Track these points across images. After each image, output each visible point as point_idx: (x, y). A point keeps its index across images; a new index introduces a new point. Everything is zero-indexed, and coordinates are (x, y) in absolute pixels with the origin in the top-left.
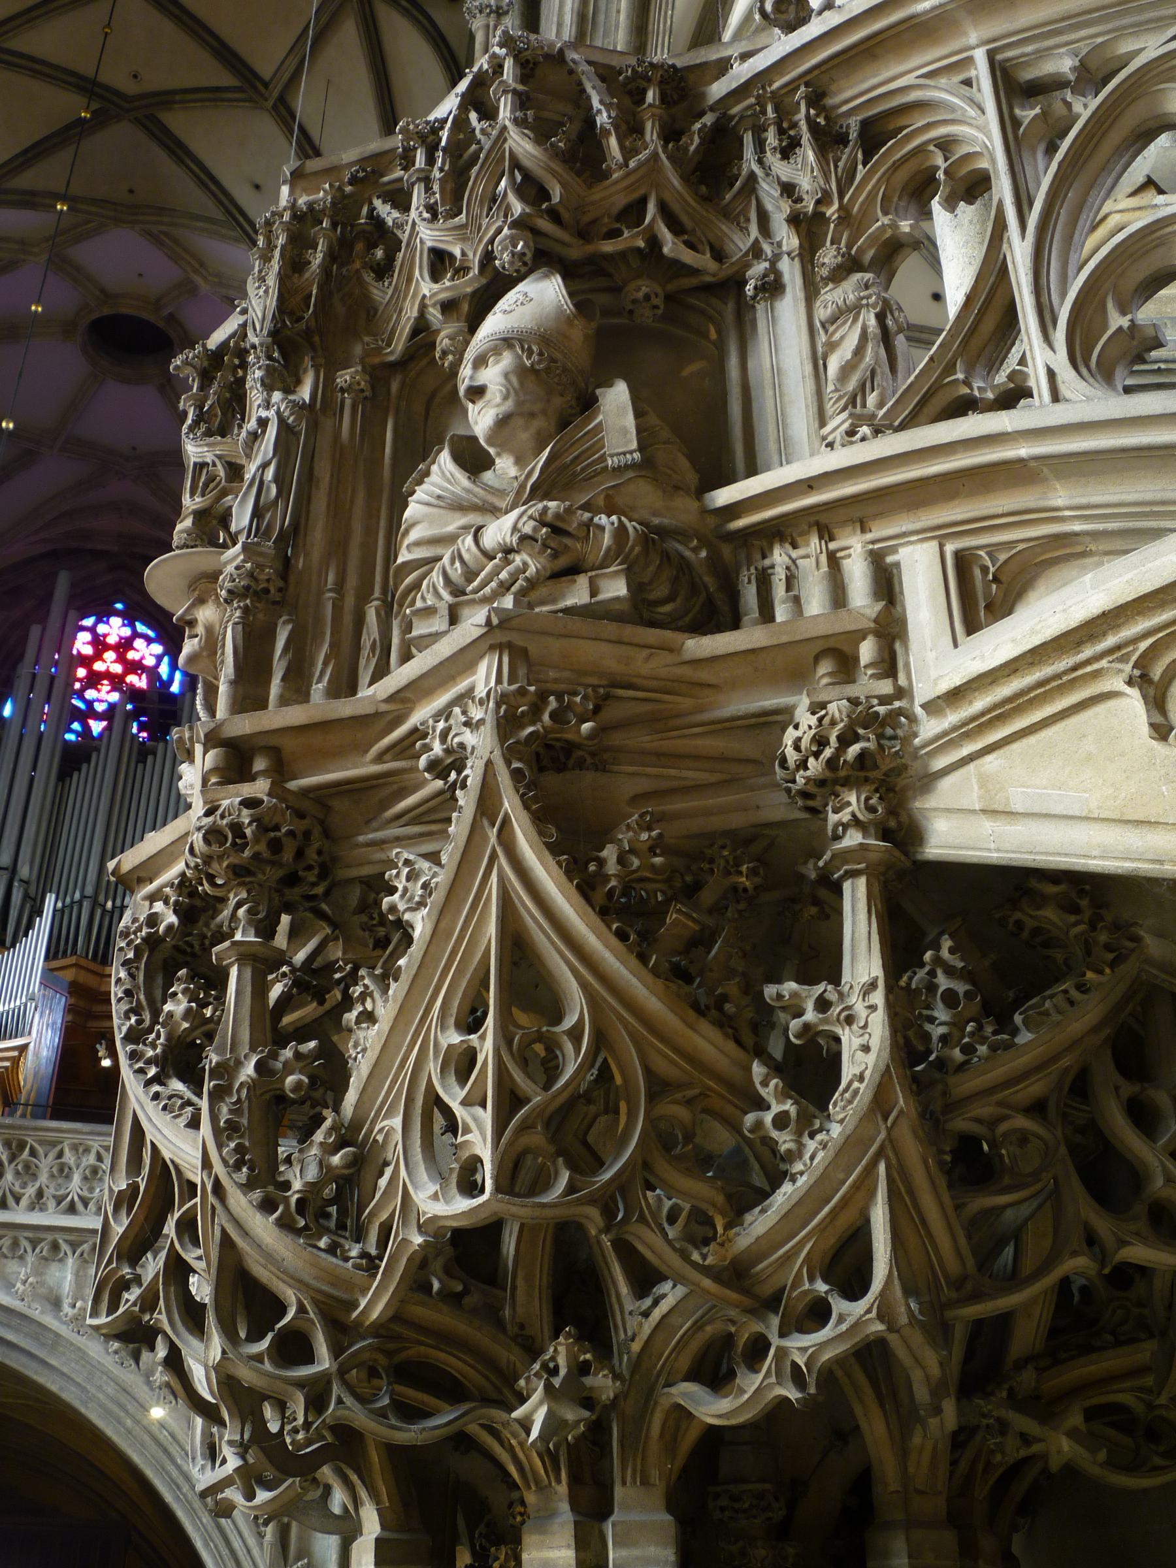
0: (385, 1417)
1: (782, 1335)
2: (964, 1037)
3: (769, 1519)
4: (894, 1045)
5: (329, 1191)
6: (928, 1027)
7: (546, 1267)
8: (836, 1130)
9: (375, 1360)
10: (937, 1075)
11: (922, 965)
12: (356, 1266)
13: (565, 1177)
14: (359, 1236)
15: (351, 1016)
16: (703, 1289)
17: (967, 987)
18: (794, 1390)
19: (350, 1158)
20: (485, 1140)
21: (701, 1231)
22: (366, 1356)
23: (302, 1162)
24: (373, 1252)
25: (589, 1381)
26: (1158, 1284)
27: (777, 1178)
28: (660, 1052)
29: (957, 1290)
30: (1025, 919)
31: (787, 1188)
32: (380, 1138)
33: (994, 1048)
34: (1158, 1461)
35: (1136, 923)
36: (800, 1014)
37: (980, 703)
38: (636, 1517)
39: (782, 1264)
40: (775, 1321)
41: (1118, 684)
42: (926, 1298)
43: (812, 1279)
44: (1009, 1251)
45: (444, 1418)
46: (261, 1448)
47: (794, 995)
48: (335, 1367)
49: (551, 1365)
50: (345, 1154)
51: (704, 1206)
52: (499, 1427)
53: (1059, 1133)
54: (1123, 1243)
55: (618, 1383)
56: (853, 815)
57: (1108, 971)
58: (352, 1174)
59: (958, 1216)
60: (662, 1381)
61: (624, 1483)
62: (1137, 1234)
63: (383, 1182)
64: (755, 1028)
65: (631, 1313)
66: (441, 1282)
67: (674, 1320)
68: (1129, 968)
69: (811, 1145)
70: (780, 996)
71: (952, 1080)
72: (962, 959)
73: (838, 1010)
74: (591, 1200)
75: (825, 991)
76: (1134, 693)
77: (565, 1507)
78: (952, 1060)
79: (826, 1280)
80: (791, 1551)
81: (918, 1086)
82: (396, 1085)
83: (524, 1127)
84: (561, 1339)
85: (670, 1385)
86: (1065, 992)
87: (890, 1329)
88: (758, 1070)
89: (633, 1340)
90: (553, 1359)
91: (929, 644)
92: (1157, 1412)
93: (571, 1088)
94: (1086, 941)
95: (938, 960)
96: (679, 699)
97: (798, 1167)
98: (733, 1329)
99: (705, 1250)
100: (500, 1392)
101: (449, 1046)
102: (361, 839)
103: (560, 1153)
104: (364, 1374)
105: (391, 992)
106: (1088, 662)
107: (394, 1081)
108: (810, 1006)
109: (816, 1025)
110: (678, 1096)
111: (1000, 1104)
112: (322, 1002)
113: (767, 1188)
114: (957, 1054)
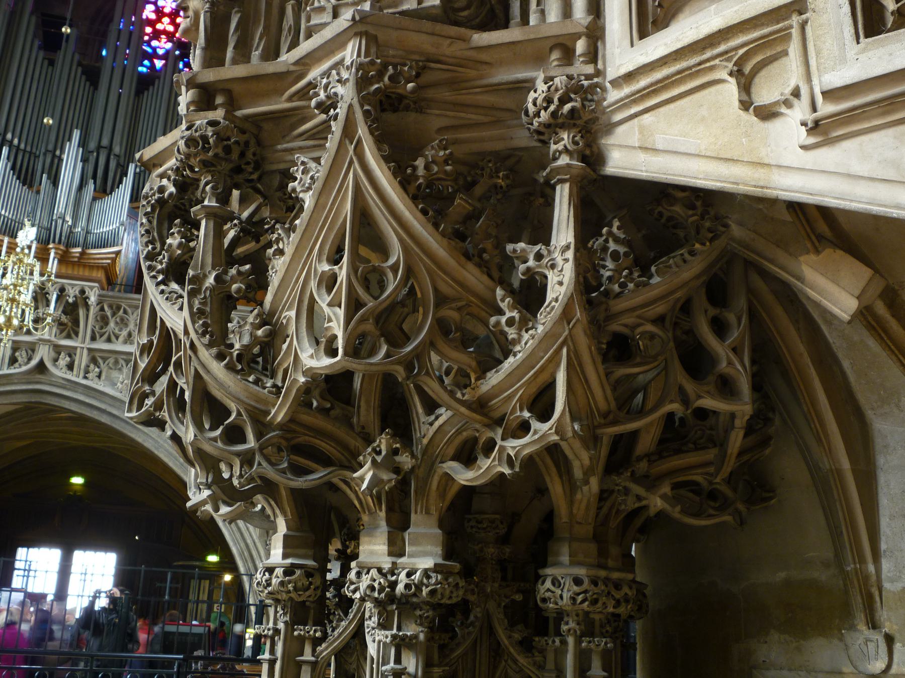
0: (285, 473)
1: (503, 439)
2: (621, 278)
3: (497, 533)
4: (577, 282)
5: (256, 350)
6: (602, 271)
7: (377, 396)
8: (540, 328)
9: (280, 443)
10: (604, 299)
11: (601, 235)
12: (270, 392)
13: (384, 349)
14: (273, 376)
15: (270, 251)
16: (461, 413)
17: (626, 249)
18: (507, 469)
19: (268, 332)
20: (339, 326)
21: (464, 381)
22: (275, 440)
23: (240, 333)
24: (280, 384)
25: (398, 458)
26: (721, 418)
27: (507, 353)
28: (444, 280)
29: (605, 418)
30: (664, 211)
31: (511, 359)
32: (284, 321)
33: (637, 285)
34: (712, 512)
35: (727, 217)
36: (526, 261)
37: (643, 82)
38: (422, 530)
39: (506, 401)
40: (500, 431)
41: (723, 74)
42: (585, 423)
43: (521, 410)
44: (640, 396)
45: (319, 475)
46: (219, 487)
47: (523, 250)
48: (257, 446)
49: (378, 449)
50: (265, 330)
51: (465, 367)
52: (349, 481)
53: (670, 335)
54: (699, 397)
55: (414, 460)
56: (565, 146)
57: (708, 244)
58: (269, 341)
59: (607, 380)
60: (439, 460)
61: (416, 513)
62: (708, 392)
63: (285, 346)
64: (500, 268)
65: (423, 423)
66: (318, 401)
67: (447, 428)
68: (721, 243)
69: (526, 336)
70: (515, 251)
71: (612, 303)
72: (624, 233)
73: (547, 260)
74: (399, 362)
75: (540, 249)
76: (733, 81)
77: (383, 523)
78: (613, 291)
79: (530, 411)
80: (508, 550)
81: (590, 304)
82: (292, 293)
83: (363, 320)
84: (383, 436)
85: (443, 462)
86: (682, 255)
87: (561, 439)
88: (499, 292)
89: (423, 437)
90: (379, 446)
91: (617, 44)
92: (714, 486)
93: (393, 296)
94: (697, 225)
95: (610, 233)
96: (468, 71)
97: (518, 348)
98: (477, 435)
99: (464, 391)
100: (349, 461)
101: (322, 272)
102: (279, 147)
103: (382, 335)
104: (275, 450)
105: (291, 239)
106: (708, 60)
107: (292, 290)
108: (531, 257)
109: (534, 268)
110: (454, 305)
111: (639, 317)
112: (258, 241)
113: (502, 358)
114: (616, 287)
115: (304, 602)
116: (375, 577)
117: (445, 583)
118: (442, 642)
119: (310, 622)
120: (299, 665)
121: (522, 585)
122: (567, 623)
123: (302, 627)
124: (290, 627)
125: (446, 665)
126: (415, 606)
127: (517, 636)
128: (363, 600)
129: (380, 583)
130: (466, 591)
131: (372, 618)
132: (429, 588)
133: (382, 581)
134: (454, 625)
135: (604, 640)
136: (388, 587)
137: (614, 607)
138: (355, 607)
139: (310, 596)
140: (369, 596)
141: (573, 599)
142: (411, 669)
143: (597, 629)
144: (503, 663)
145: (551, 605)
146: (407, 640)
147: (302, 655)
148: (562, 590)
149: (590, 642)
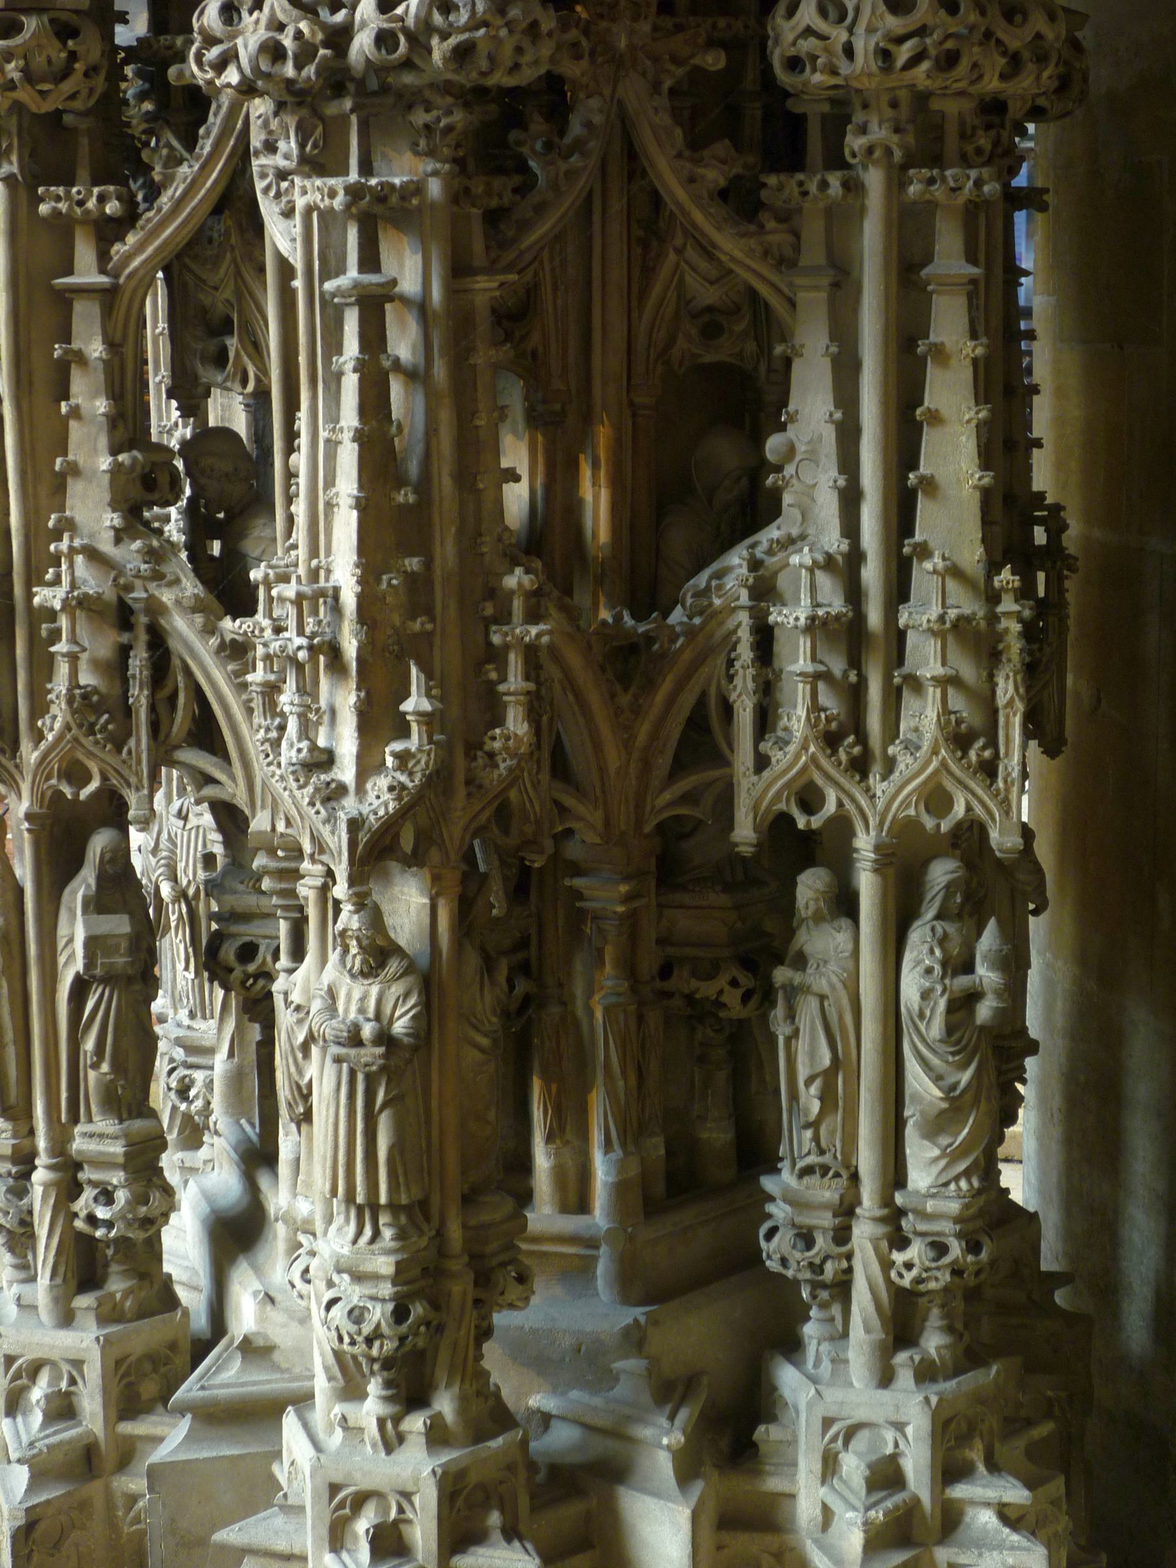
115: (58, 114)
116: (281, 17)
117: (499, 21)
118: (494, 203)
119: (83, 173)
120: (64, 300)
121: (722, 23)
122: (863, 130)
123: (61, 191)
124: (23, 194)
125: (508, 269)
126: (409, 101)
127: (714, 176)
128: (248, 89)
129: (299, 35)
130: (559, 47)
131: (282, 145)
132: (453, 41)
133: (304, 26)
134: (525, 150)
135: (973, 174)
136: (326, 44)
137: (1003, 77)
138: (215, 121)
139: (73, 97)
140: (268, 76)
141: (885, 55)
142: (410, 284)
143: (952, 144)
144: (672, 257)
145: (817, 78)
146: (394, 200)
147: (70, 272)
148: (851, 30)
149: (931, 181)
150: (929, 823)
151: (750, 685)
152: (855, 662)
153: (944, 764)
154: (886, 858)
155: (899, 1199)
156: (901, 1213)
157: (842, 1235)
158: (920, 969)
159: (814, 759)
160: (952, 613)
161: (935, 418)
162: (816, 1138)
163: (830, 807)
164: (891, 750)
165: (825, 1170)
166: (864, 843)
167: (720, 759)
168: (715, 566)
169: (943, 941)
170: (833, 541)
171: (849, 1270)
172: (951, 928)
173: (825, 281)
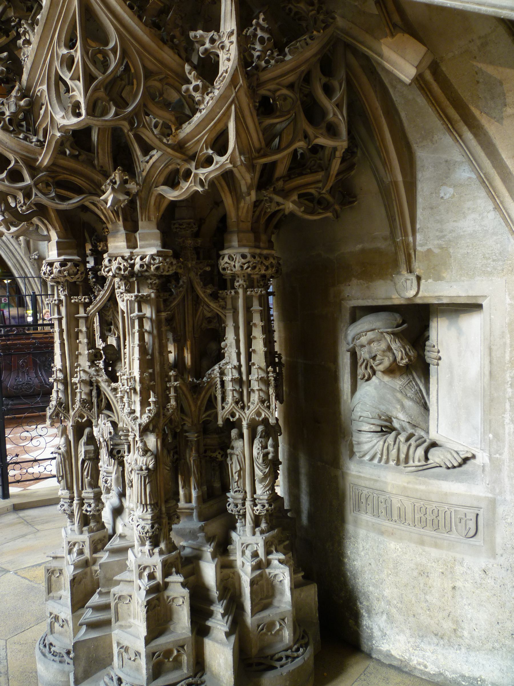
0: (54, 200)
1: (196, 169)
2: (266, 57)
3: (192, 231)
4: (239, 58)
5: (21, 116)
6: (253, 52)
7: (109, 145)
8: (216, 92)
9: (48, 180)
10: (255, 72)
11: (252, 26)
12: (36, 145)
13: (113, 110)
14: (36, 133)
15: (20, 42)
16: (167, 152)
17: (269, 36)
18: (200, 188)
19: (28, 102)
20: (81, 94)
21: (167, 131)
22: (44, 178)
23: (8, 104)
24: (42, 139)
25: (127, 186)
26: (327, 152)
27: (194, 111)
28: (148, 59)
29: (258, 153)
30: (292, 7)
31: (198, 115)
32: (39, 94)
33: (277, 62)
34: (321, 211)
35: (334, 11)
36: (203, 45)
38: (147, 231)
39: (196, 143)
40: (194, 164)
42: (247, 156)
43: (207, 149)
44: (277, 140)
45: (76, 200)
46: (10, 212)
47: (201, 36)
48: (33, 183)
49: (114, 181)
50: (26, 101)
51: (168, 122)
52: (96, 203)
53: (298, 96)
54: (316, 137)
55: (138, 186)
57: (322, 31)
58: (29, 109)
59: (260, 126)
60: (154, 185)
61: (142, 220)
62: (322, 134)
63: (42, 112)
64: (186, 50)
65: (142, 162)
66: (69, 150)
67: (158, 164)
68: (330, 30)
69: (207, 98)
70: (196, 37)
71: (261, 74)
72: (267, 24)
73: (218, 43)
74: (124, 119)
75: (213, 35)
77: (122, 229)
78: (261, 66)
79: (212, 149)
80: (199, 241)
81: (248, 76)
82: (42, 72)
83: (96, 89)
84: (117, 171)
85: (157, 187)
86: (305, 39)
87: (234, 166)
88: (187, 67)
89: (143, 171)
90: (114, 178)
92: (322, 195)
93: (114, 73)
94: (315, 18)
95: (258, 24)
97: (202, 106)
98: (179, 167)
99: (168, 138)
100: (95, 190)
101: (63, 55)
103: (111, 100)
104: (44, 186)
105: (35, 31)
107: (42, 70)
108: (207, 41)
109: (210, 49)
110: (157, 77)
111: (278, 84)
112: (8, 36)
113: (191, 115)
114: (263, 63)
115: (75, 282)
116: (120, 262)
117: (164, 262)
118: (165, 298)
119: (81, 294)
120: (77, 320)
121: (209, 261)
122: (238, 282)
123: (76, 297)
124: (68, 298)
125: (168, 311)
126: (147, 278)
127: (209, 291)
128: (114, 276)
129: (124, 265)
130: (177, 267)
131: (121, 287)
132: (155, 266)
133: (125, 264)
134: (171, 287)
135: (260, 289)
136: (130, 267)
137: (265, 271)
138: (108, 283)
139: (78, 278)
140: (118, 274)
141: (242, 267)
142: (148, 314)
143: (256, 284)
144: (201, 308)
145: (229, 272)
146: (144, 298)
147: (78, 314)
148: (235, 262)
149: (252, 291)
150: (257, 419)
151: (220, 392)
152: (241, 387)
153: (260, 407)
154: (249, 426)
155: (255, 496)
156: (255, 499)
157: (244, 504)
158: (257, 448)
159: (233, 407)
160: (260, 376)
161: (255, 338)
162: (237, 485)
163: (237, 416)
164: (249, 404)
165: (239, 491)
166: (244, 423)
167: (215, 407)
168: (212, 369)
169: (261, 442)
170: (236, 363)
171: (245, 512)
172: (263, 440)
173: (232, 311)
